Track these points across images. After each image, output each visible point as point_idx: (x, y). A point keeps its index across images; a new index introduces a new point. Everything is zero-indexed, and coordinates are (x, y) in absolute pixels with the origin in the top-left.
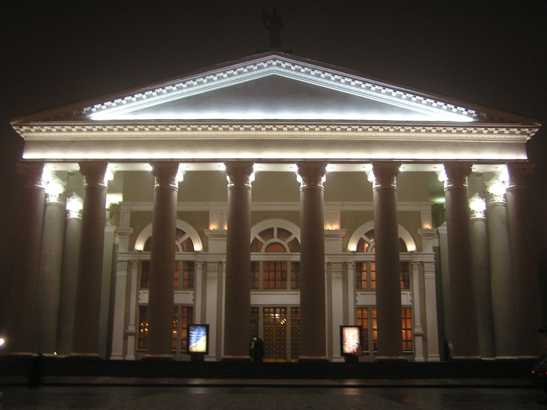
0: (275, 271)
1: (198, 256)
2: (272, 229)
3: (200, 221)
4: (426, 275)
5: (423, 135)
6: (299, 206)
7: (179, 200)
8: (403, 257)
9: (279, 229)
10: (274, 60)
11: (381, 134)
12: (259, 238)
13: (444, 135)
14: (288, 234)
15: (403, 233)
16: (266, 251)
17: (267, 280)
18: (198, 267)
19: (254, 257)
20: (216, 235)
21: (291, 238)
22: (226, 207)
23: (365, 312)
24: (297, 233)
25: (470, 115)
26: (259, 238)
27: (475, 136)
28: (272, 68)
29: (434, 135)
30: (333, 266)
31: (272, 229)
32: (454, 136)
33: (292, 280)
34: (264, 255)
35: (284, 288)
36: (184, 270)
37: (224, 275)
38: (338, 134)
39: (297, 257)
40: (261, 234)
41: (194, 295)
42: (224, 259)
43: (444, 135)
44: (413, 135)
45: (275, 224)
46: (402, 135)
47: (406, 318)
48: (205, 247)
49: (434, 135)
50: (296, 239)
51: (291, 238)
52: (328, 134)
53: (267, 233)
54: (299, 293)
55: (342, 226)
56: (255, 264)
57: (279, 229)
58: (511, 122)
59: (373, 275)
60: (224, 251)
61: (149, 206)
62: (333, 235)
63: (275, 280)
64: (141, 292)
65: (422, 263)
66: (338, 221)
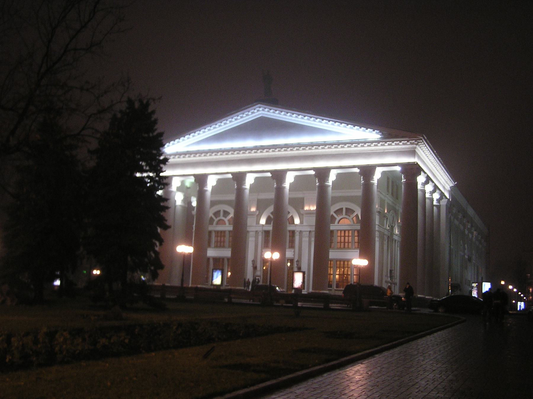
0: (345, 236)
2: (342, 209)
3: (298, 204)
4: (304, 239)
5: (346, 149)
6: (359, 192)
7: (290, 190)
8: (290, 228)
9: (347, 209)
10: (260, 107)
11: (320, 151)
12: (214, 218)
13: (359, 149)
14: (353, 211)
15: (293, 212)
16: (217, 224)
17: (217, 242)
19: (211, 228)
20: (309, 213)
21: (355, 214)
22: (315, 194)
23: (338, 263)
24: (358, 211)
26: (335, 215)
27: (380, 147)
28: (260, 112)
29: (353, 149)
30: (304, 233)
31: (219, 211)
32: (366, 148)
33: (289, 242)
35: (224, 247)
36: (230, 236)
37: (313, 239)
38: (295, 152)
39: (231, 228)
40: (335, 212)
41: (294, 252)
42: (313, 229)
43: (359, 149)
44: (340, 150)
45: (344, 205)
46: (333, 150)
47: (330, 267)
48: (301, 222)
49: (353, 149)
50: (357, 216)
51: (355, 214)
52: (289, 153)
53: (217, 214)
54: (358, 251)
55: (258, 209)
56: (332, 232)
57: (347, 209)
59: (356, 238)
60: (314, 224)
61: (271, 195)
62: (253, 214)
63: (344, 242)
65: (301, 232)
66: (256, 206)
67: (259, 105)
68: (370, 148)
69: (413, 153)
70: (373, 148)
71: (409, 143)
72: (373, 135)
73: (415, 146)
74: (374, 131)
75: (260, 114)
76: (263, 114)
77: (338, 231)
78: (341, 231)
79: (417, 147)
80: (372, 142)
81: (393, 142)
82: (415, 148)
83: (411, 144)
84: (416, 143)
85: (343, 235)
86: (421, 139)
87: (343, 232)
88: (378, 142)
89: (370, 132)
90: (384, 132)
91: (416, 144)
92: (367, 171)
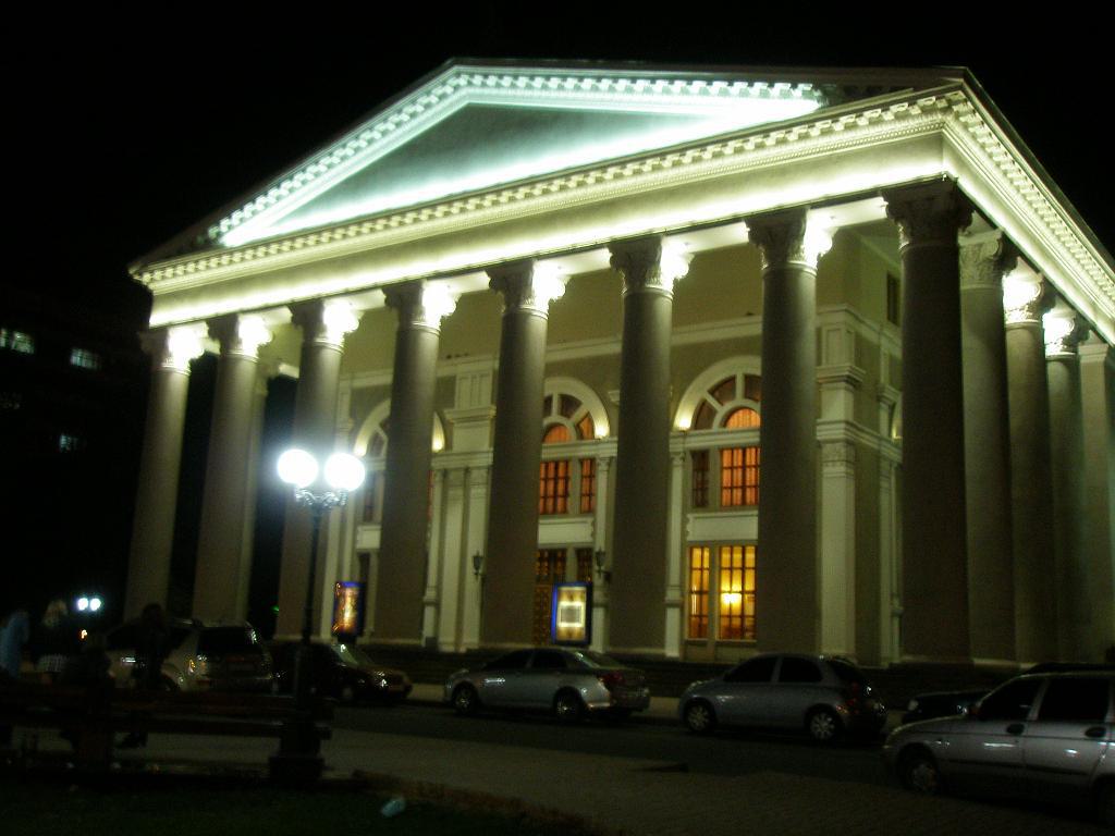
1: (600, 446)
10: (458, 75)
18: (600, 468)
25: (806, 94)
28: (463, 92)
34: (719, 433)
58: (894, 89)
64: (690, 516)
67: (455, 69)
68: (784, 150)
69: (936, 142)
70: (795, 148)
71: (915, 110)
72: (791, 100)
73: (939, 117)
74: (794, 86)
75: (464, 97)
76: (471, 96)
77: (721, 450)
78: (732, 449)
79: (949, 119)
80: (788, 126)
81: (859, 113)
82: (942, 125)
83: (926, 111)
84: (942, 104)
85: (738, 461)
86: (961, 88)
87: (738, 455)
88: (809, 121)
89: (784, 95)
90: (830, 87)
91: (947, 110)
92: (776, 231)
